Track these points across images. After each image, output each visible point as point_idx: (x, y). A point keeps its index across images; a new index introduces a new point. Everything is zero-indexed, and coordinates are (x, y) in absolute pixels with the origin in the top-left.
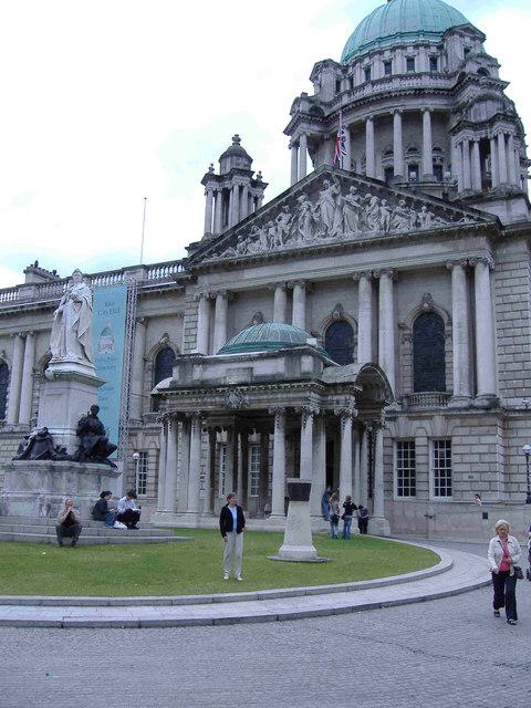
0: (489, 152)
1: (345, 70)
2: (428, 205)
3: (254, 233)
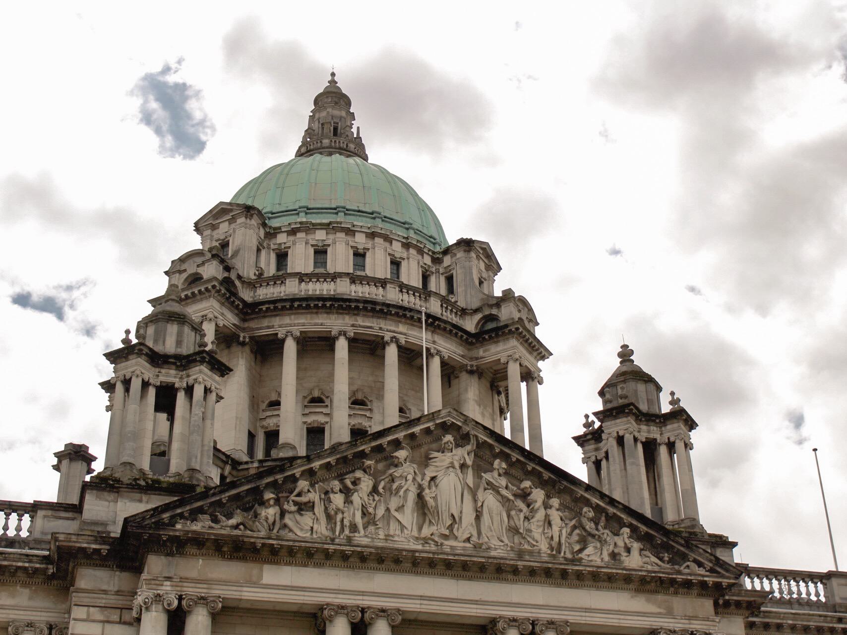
1: (272, 234)
2: (630, 526)
3: (299, 495)
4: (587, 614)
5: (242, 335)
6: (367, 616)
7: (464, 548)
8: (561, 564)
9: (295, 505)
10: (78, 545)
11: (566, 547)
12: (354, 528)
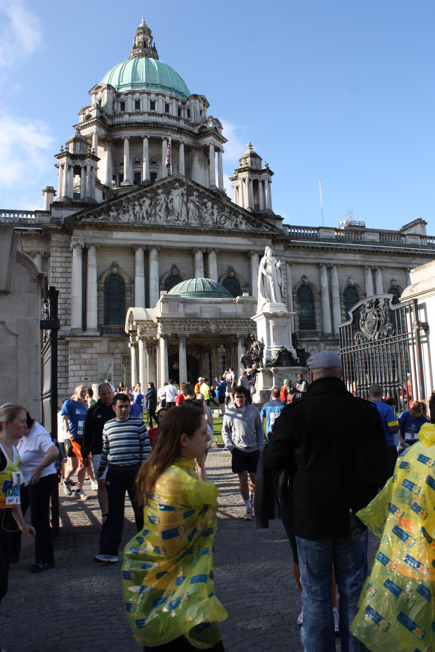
2: (243, 215)
3: (124, 207)
6: (148, 248)
7: (183, 224)
12: (143, 218)
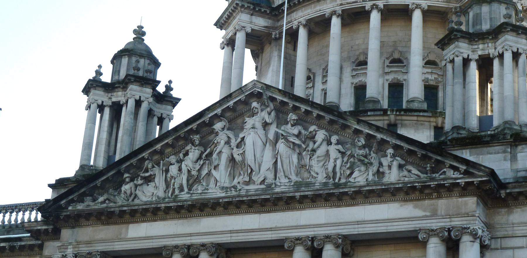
0: (492, 75)
2: (396, 147)
3: (147, 171)
4: (359, 226)
5: (274, 33)
7: (257, 190)
8: (330, 189)
9: (141, 180)
10: (36, 228)
11: (341, 174)
12: (181, 189)
